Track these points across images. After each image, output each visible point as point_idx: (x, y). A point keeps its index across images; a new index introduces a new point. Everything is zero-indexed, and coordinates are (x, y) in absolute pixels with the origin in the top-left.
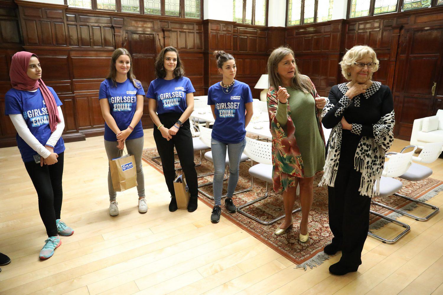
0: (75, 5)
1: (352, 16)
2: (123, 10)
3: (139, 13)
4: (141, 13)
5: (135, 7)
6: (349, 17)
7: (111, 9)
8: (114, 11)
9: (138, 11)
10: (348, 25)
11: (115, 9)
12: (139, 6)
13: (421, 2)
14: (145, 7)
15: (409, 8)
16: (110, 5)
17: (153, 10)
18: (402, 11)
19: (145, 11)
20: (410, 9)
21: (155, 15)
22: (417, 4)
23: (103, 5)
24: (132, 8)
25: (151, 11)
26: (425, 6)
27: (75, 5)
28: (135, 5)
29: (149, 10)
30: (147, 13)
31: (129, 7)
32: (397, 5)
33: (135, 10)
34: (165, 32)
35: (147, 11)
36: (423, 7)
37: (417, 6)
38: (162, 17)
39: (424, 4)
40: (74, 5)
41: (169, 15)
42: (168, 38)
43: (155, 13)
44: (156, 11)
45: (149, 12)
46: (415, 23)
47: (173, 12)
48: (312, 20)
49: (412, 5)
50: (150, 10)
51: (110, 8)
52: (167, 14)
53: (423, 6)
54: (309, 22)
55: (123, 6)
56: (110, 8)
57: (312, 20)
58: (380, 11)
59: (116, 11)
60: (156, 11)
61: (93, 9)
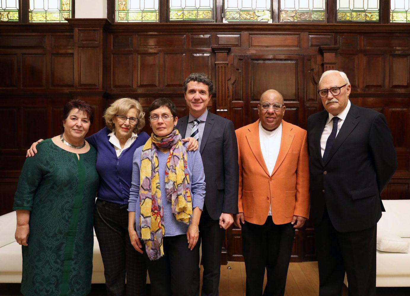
1: (120, 18)
6: (114, 19)
10: (112, 35)
13: (254, 13)
15: (236, 19)
18: (225, 22)
20: (238, 20)
22: (249, 14)
26: (262, 19)
32: (213, 9)
36: (259, 20)
37: (248, 17)
39: (259, 16)
46: (251, 45)
48: (15, 17)
49: (240, 15)
53: (259, 19)
54: (5, 19)
57: (15, 17)
58: (181, 17)
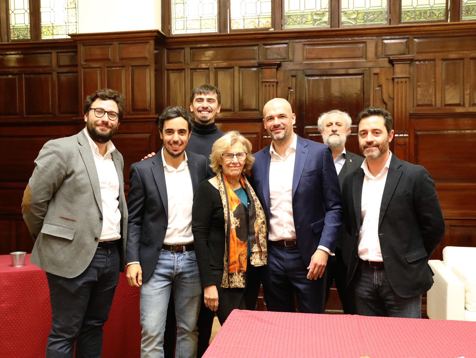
0: (185, 29)
2: (288, 24)
3: (326, 26)
4: (331, 27)
5: (317, 13)
7: (261, 26)
8: (267, 29)
9: (325, 22)
11: (270, 26)
12: (327, 10)
14: (342, 10)
16: (259, 18)
17: (366, 13)
19: (344, 19)
21: (370, 25)
23: (244, 19)
24: (310, 17)
25: (360, 15)
27: (185, 29)
28: (318, 8)
29: (354, 16)
30: (349, 23)
31: (303, 16)
33: (315, 20)
34: (396, 66)
35: (349, 19)
38: (391, 26)
40: (184, 29)
41: (412, 20)
42: (404, 80)
43: (372, 21)
44: (373, 15)
45: (355, 19)
47: (425, 12)
50: (358, 14)
51: (259, 24)
52: (406, 19)
55: (289, 16)
56: (259, 24)
59: (272, 30)
60: (373, 15)
61: (220, 32)
